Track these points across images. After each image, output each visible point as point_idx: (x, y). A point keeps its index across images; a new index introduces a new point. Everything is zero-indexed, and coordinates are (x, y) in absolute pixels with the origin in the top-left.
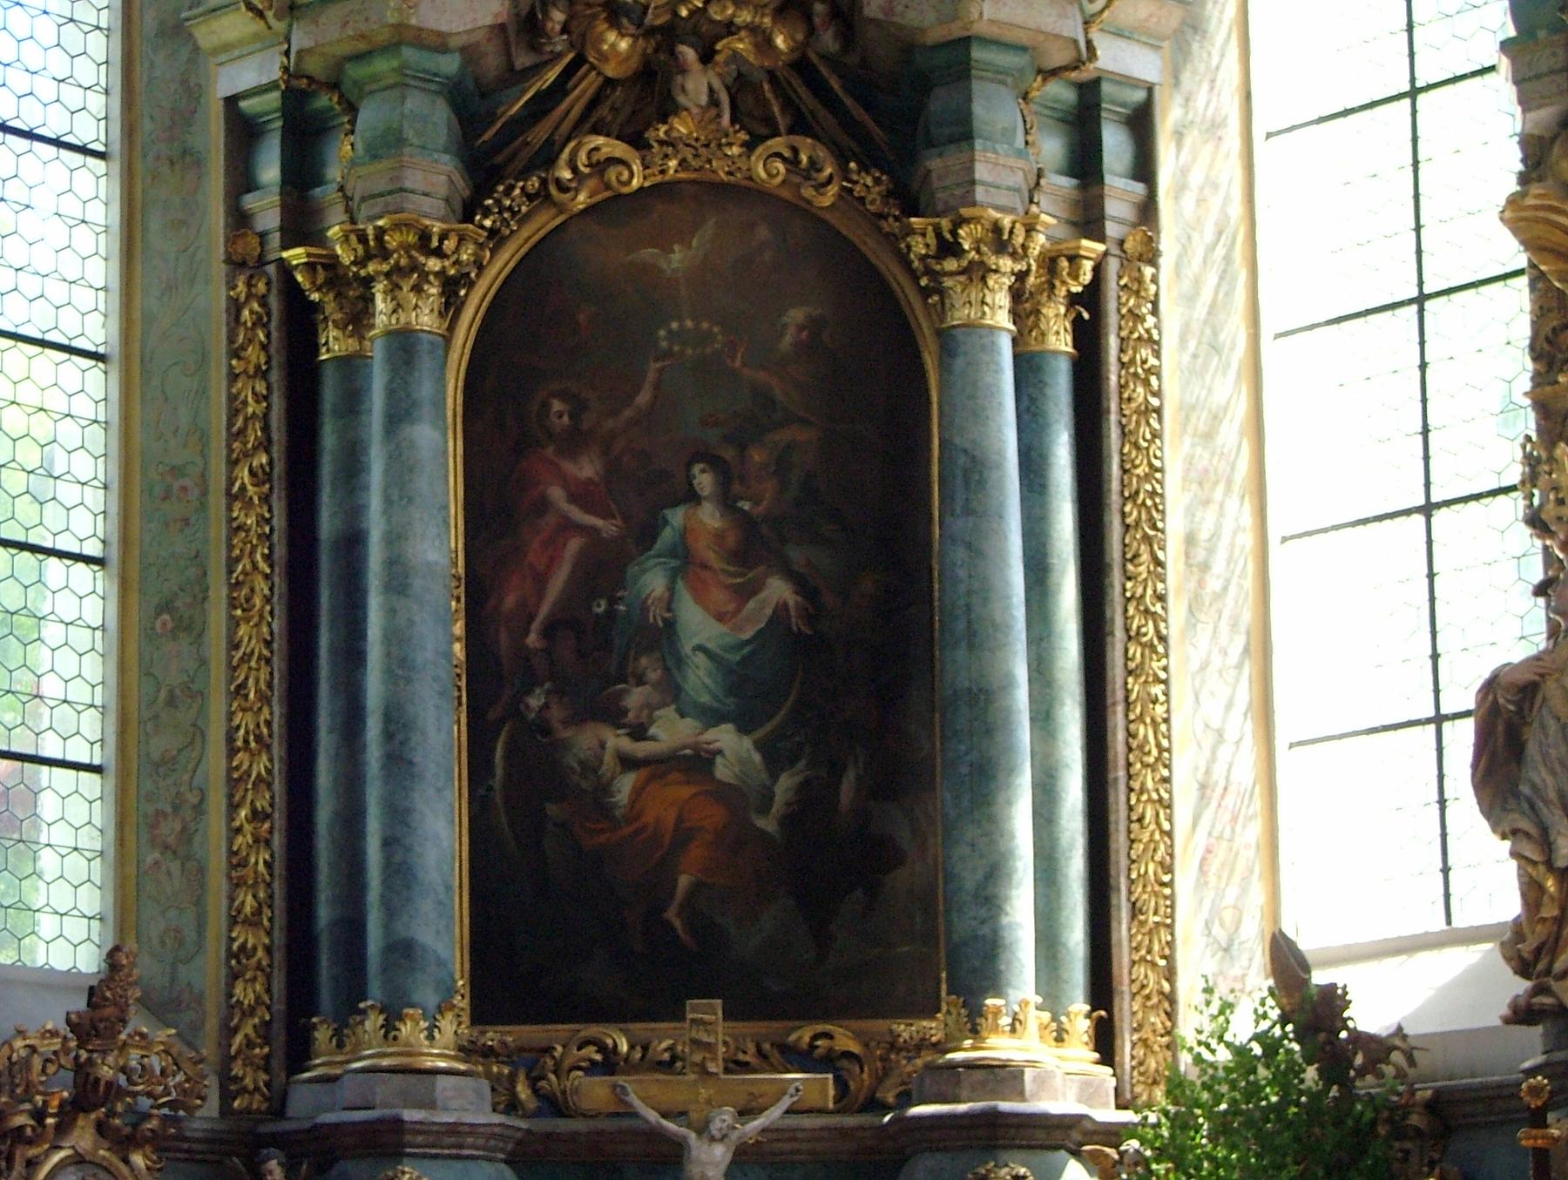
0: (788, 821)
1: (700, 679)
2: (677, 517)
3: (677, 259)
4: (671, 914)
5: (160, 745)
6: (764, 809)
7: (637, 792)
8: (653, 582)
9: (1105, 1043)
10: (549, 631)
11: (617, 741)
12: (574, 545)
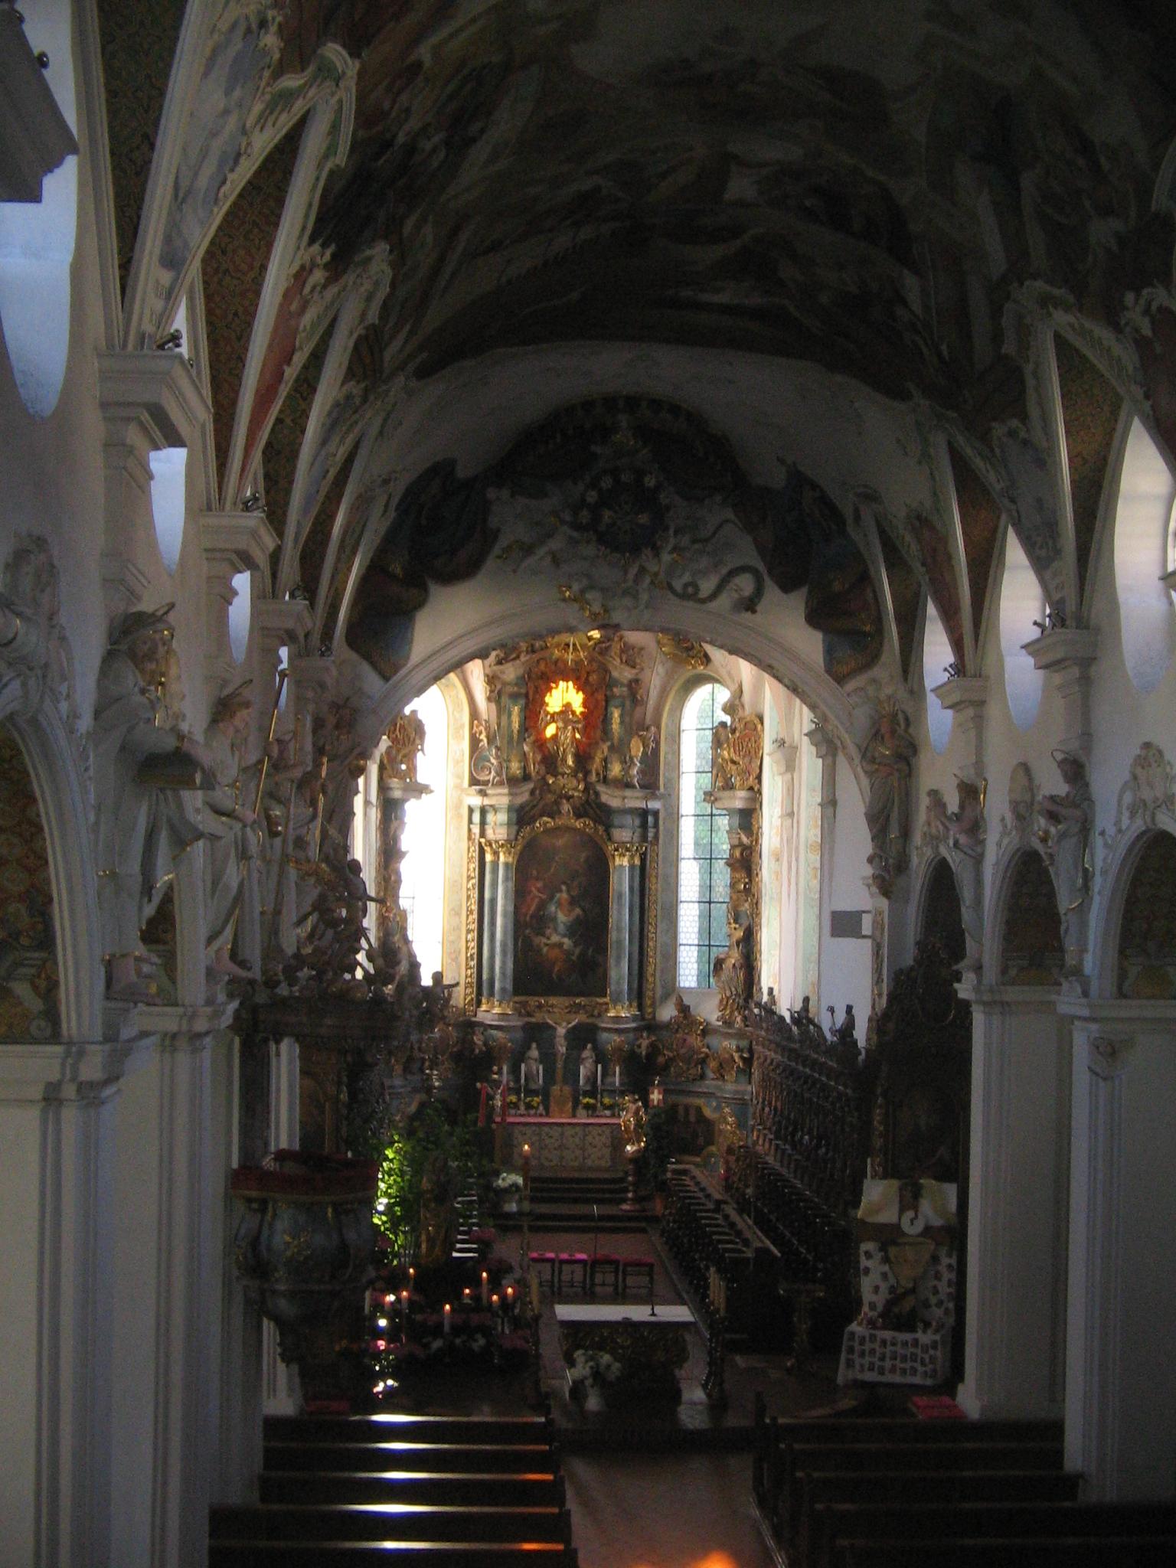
0: (578, 958)
1: (561, 928)
2: (558, 895)
3: (560, 842)
4: (554, 976)
5: (452, 938)
6: (573, 955)
7: (548, 951)
8: (553, 909)
9: (640, 1007)
10: (531, 917)
11: (544, 940)
12: (537, 900)
